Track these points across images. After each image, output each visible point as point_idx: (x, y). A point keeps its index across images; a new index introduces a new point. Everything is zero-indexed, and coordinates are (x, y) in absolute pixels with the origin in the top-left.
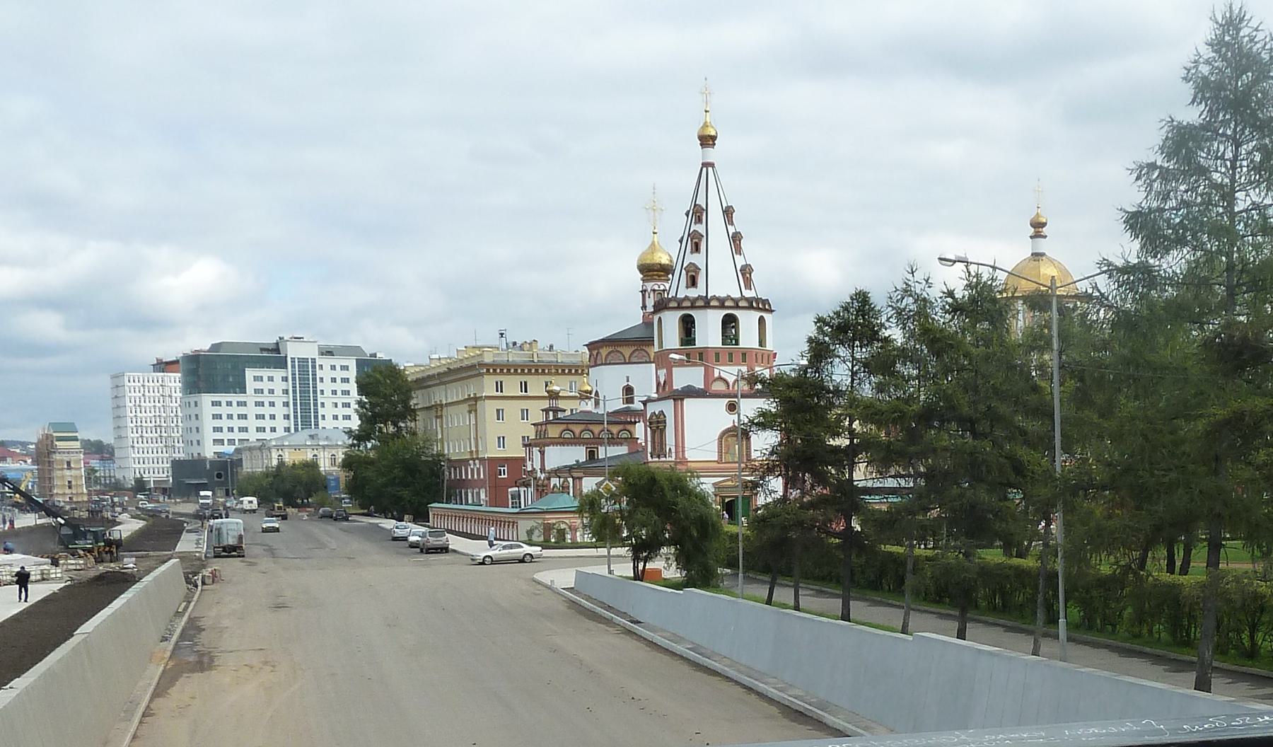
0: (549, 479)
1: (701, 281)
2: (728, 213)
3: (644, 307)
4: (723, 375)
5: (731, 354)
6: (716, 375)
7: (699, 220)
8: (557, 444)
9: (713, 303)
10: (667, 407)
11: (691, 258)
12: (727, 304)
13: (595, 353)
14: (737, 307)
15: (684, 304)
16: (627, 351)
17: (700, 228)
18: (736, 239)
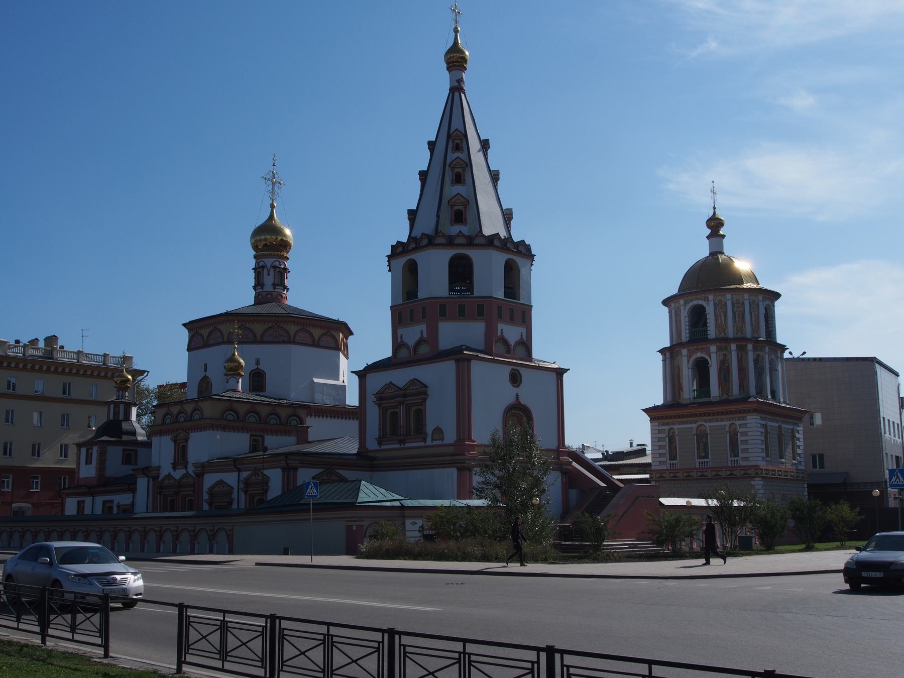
0: (200, 476)
3: (259, 283)
4: (507, 336)
5: (512, 310)
7: (457, 148)
8: (214, 427)
9: (496, 243)
10: (438, 377)
11: (453, 190)
13: (205, 332)
14: (519, 253)
16: (258, 328)
18: (495, 177)
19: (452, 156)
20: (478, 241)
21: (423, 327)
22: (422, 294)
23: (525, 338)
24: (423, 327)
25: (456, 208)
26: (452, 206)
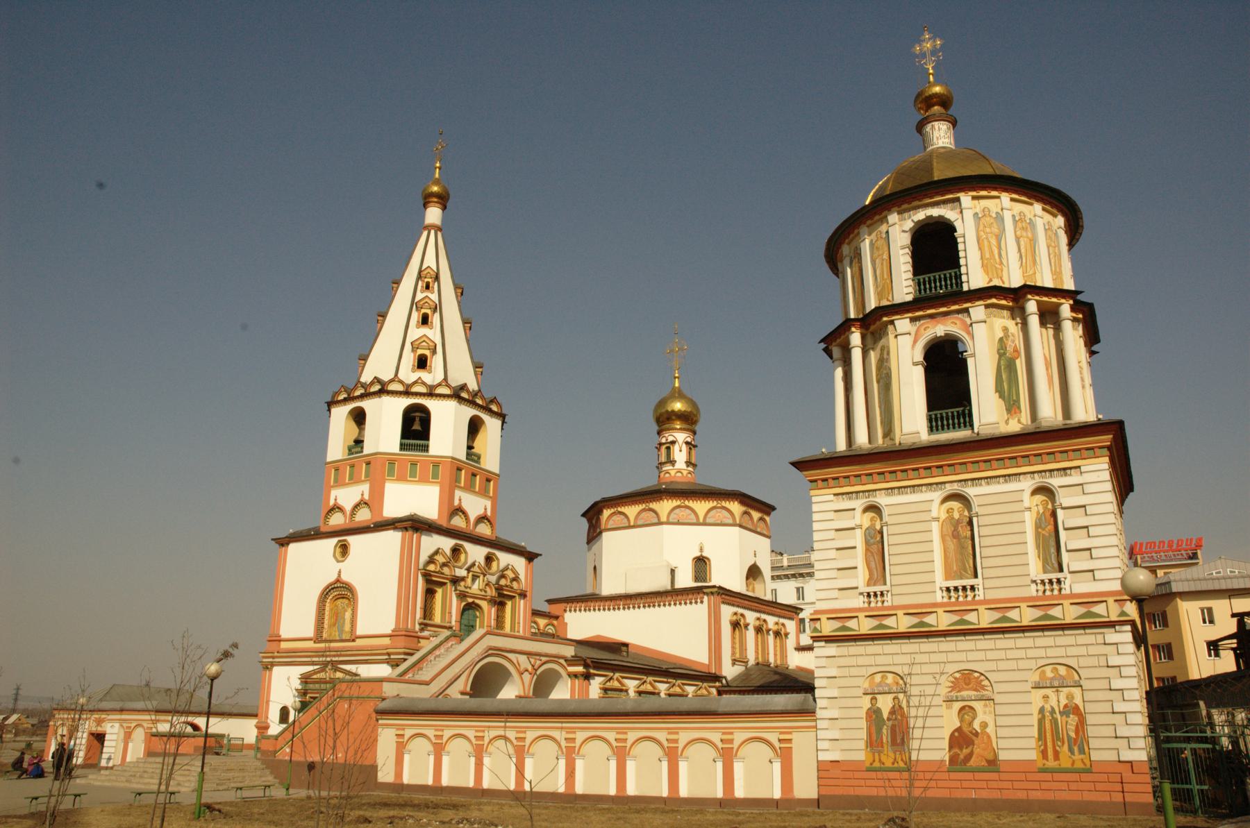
1: (436, 362)
2: (460, 290)
4: (465, 506)
6: (456, 503)
11: (416, 332)
12: (479, 401)
14: (490, 412)
15: (416, 389)
17: (434, 297)
19: (419, 296)
20: (439, 391)
21: (365, 488)
22: (366, 451)
23: (489, 513)
24: (365, 488)
25: (420, 352)
26: (414, 349)
